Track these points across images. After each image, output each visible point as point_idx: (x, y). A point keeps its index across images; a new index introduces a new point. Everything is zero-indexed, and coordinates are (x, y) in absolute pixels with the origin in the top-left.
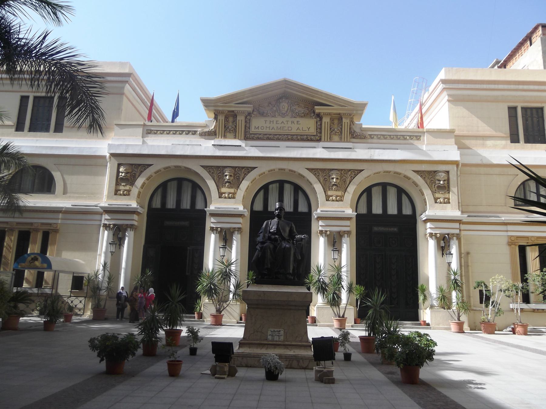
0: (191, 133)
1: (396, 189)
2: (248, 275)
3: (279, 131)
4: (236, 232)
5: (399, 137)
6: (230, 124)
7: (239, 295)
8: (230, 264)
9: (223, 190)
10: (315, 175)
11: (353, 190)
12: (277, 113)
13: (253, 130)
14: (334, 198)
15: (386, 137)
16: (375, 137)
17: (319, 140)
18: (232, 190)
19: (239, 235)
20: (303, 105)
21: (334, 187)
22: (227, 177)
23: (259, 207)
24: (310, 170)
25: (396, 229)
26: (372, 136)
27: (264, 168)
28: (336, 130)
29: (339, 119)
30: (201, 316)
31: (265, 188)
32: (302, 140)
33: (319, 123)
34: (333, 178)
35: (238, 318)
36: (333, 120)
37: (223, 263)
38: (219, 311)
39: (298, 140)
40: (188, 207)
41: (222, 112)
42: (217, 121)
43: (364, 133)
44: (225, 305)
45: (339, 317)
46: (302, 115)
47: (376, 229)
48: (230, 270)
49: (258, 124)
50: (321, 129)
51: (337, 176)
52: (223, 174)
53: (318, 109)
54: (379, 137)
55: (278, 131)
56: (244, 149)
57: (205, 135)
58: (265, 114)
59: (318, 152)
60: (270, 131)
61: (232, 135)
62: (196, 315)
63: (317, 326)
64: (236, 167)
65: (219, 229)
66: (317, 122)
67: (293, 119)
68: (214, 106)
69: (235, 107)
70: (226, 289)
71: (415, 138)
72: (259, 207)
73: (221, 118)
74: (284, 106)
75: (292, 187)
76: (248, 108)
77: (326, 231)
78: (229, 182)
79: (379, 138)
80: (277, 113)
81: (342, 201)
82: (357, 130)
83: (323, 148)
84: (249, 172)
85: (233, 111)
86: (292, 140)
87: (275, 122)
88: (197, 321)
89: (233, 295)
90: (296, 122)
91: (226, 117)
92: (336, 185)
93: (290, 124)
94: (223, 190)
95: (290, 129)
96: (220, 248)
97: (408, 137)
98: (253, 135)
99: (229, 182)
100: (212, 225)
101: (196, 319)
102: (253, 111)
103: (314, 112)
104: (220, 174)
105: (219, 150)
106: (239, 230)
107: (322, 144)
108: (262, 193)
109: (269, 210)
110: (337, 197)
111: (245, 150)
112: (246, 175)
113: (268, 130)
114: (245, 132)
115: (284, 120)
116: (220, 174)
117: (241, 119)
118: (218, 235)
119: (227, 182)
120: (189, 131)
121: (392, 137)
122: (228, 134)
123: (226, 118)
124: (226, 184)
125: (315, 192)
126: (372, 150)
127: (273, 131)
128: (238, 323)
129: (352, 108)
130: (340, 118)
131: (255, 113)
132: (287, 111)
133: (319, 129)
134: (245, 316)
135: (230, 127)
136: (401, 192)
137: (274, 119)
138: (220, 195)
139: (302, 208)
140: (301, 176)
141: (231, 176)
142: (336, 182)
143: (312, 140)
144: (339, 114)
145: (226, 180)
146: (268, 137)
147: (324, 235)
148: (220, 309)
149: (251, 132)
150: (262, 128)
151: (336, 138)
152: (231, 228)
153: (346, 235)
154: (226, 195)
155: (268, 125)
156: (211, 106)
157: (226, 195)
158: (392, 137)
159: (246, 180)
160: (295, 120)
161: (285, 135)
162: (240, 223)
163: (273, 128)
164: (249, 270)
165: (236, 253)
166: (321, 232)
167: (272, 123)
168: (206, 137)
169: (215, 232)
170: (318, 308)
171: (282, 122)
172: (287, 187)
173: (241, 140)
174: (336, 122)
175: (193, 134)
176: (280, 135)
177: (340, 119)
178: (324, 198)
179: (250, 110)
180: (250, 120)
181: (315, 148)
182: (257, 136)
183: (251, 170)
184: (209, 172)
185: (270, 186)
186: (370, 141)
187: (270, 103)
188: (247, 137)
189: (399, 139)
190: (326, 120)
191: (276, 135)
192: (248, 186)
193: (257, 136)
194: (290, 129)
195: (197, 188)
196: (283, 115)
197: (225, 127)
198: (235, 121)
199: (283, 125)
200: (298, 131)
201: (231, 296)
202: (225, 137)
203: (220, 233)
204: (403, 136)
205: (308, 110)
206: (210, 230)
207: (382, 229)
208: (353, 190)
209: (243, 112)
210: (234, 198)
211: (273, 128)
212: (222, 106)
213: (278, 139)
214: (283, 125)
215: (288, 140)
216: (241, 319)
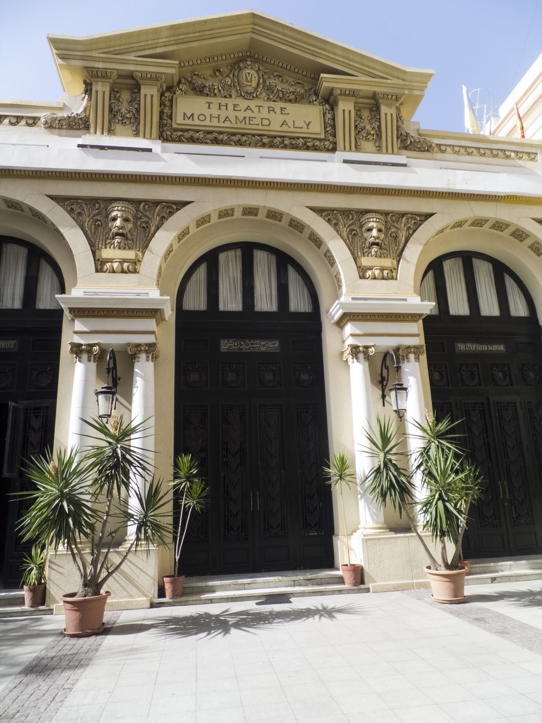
0: (23, 122)
1: (490, 265)
2: (176, 465)
3: (242, 125)
4: (143, 356)
5: (495, 152)
6: (124, 108)
7: (157, 527)
8: (127, 433)
9: (106, 253)
10: (329, 221)
11: (415, 256)
12: (234, 93)
13: (179, 120)
14: (377, 273)
15: (470, 150)
16: (449, 149)
17: (334, 150)
18: (130, 254)
19: (151, 364)
20: (290, 79)
21: (375, 249)
22: (118, 222)
23: (197, 301)
24: (319, 211)
25: (501, 348)
26: (443, 148)
27: (210, 202)
28: (368, 127)
29: (371, 110)
30: (40, 596)
31: (211, 259)
32: (295, 147)
33: (329, 116)
34: (370, 230)
35: (154, 591)
36: (359, 110)
37: (103, 429)
38: (93, 584)
39: (285, 147)
40: (18, 305)
41: (103, 75)
42: (90, 96)
43: (428, 139)
44: (115, 558)
45: (448, 567)
46: (292, 97)
47: (461, 347)
48: (128, 450)
49: (190, 109)
50: (334, 127)
51: (379, 225)
52: (107, 216)
53: (328, 81)
54: (456, 150)
55: (239, 125)
56: (158, 159)
57: (61, 128)
58: (206, 91)
59: (330, 169)
60: (221, 124)
61: (129, 129)
62: (25, 593)
63: (367, 590)
64: (139, 202)
65: (96, 348)
66: (324, 114)
67: (272, 104)
68: (83, 58)
69: (137, 64)
70: (114, 510)
71: (525, 156)
72: (197, 301)
73: (102, 88)
74: (250, 76)
75: (273, 258)
76: (169, 69)
77: (367, 347)
78: (122, 235)
79: (457, 153)
80: (234, 93)
81: (392, 278)
82: (412, 134)
83: (345, 161)
84: (171, 214)
85: (131, 76)
86: (272, 146)
87: (231, 107)
88: (31, 613)
89: (139, 530)
90: (278, 110)
91: (112, 90)
92: (377, 244)
93: (264, 113)
94: (106, 253)
95: (266, 122)
96: (97, 394)
97: (513, 154)
98: (179, 133)
99: (122, 235)
100: (77, 339)
101: (26, 607)
102: (179, 82)
103: (316, 94)
104: (98, 218)
105: (96, 157)
106: (151, 349)
107: (340, 155)
108: (202, 272)
109: (221, 308)
110: (382, 270)
111: (161, 159)
112: (163, 219)
113: (215, 123)
114: (162, 126)
115: (253, 104)
116: (98, 218)
117: (150, 92)
118: (93, 365)
119: (117, 234)
120: (19, 119)
121: (482, 151)
122: (119, 128)
123: (114, 92)
124: (113, 238)
125: (332, 262)
126: (450, 171)
127: (227, 124)
128: (153, 605)
129: (401, 82)
130: (373, 104)
131: (183, 87)
132: (256, 89)
133: (331, 126)
134: (173, 583)
135: (123, 110)
136: (501, 271)
137: (230, 102)
138: (100, 266)
139: (298, 303)
140: (297, 226)
141: (126, 220)
142: (378, 238)
143: (315, 149)
144: (374, 96)
145: (114, 230)
146: (216, 138)
147: (361, 356)
148: (95, 576)
149: (174, 126)
150: (202, 118)
151: (369, 145)
152: (128, 344)
153: (412, 356)
154: (116, 265)
155: (214, 111)
156: (74, 58)
157: (116, 265)
158: (482, 151)
159: (167, 230)
160: (278, 105)
161: (254, 135)
162: (153, 333)
163: (227, 119)
164: (178, 452)
165: (147, 404)
166: (355, 350)
167: (223, 108)
168: (64, 132)
169: (85, 356)
170: (366, 541)
171: (248, 108)
172: (261, 259)
173: (151, 138)
174: (366, 114)
175: (28, 124)
176: (243, 135)
177: (375, 109)
178: (355, 273)
179: (172, 71)
180: (171, 101)
181: (326, 161)
182: (191, 133)
183: (178, 210)
184: (71, 212)
185: (222, 257)
186: (439, 155)
187: (219, 71)
188: (168, 133)
189: (496, 156)
190: (345, 106)
191: (234, 134)
192: (171, 246)
193: (191, 133)
194: (266, 122)
195: (42, 261)
196: (249, 96)
197: (111, 110)
198: (135, 100)
199: (248, 114)
200: (285, 128)
201: (132, 529)
202: (111, 132)
203: (100, 358)
204: (504, 151)
205: (303, 87)
206: (72, 351)
207: (472, 347)
208: (415, 256)
209: (155, 78)
210: (135, 271)
211: (227, 119)
212: (103, 60)
213: (239, 143)
214: (248, 114)
215: (264, 145)
216: (161, 593)
